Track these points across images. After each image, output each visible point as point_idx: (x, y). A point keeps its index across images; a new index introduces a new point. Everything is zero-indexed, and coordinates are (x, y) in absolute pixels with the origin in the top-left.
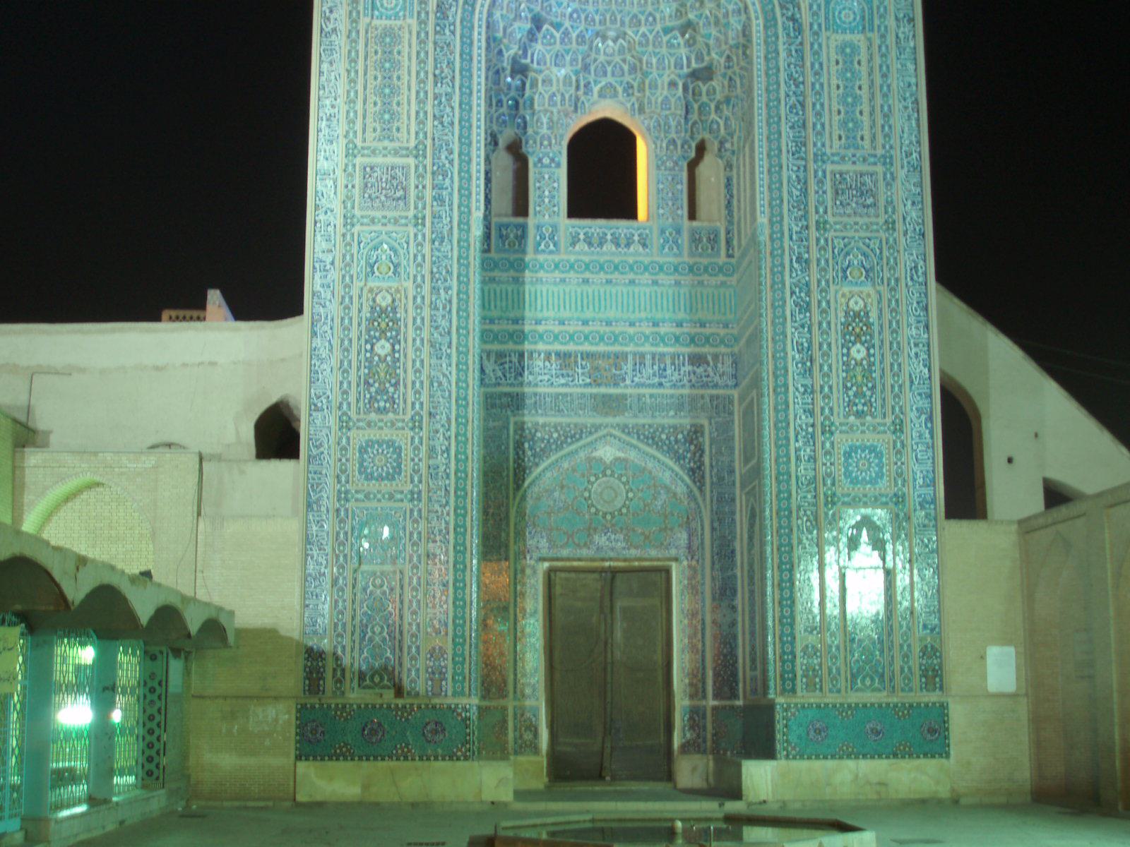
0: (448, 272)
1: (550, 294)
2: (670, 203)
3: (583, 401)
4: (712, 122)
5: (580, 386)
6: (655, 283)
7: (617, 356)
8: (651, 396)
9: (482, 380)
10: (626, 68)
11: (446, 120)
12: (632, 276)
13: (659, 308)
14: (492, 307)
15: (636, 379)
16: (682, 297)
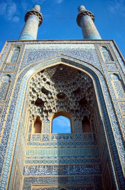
0: (9, 128)
1: (46, 151)
2: (78, 129)
3: (54, 179)
4: (87, 112)
5: (54, 175)
6: (75, 147)
7: (65, 166)
8: (76, 177)
9: (24, 173)
10: (65, 102)
11: (15, 97)
12: (68, 146)
13: (77, 153)
14: (29, 154)
15: (71, 172)
16: (83, 150)
